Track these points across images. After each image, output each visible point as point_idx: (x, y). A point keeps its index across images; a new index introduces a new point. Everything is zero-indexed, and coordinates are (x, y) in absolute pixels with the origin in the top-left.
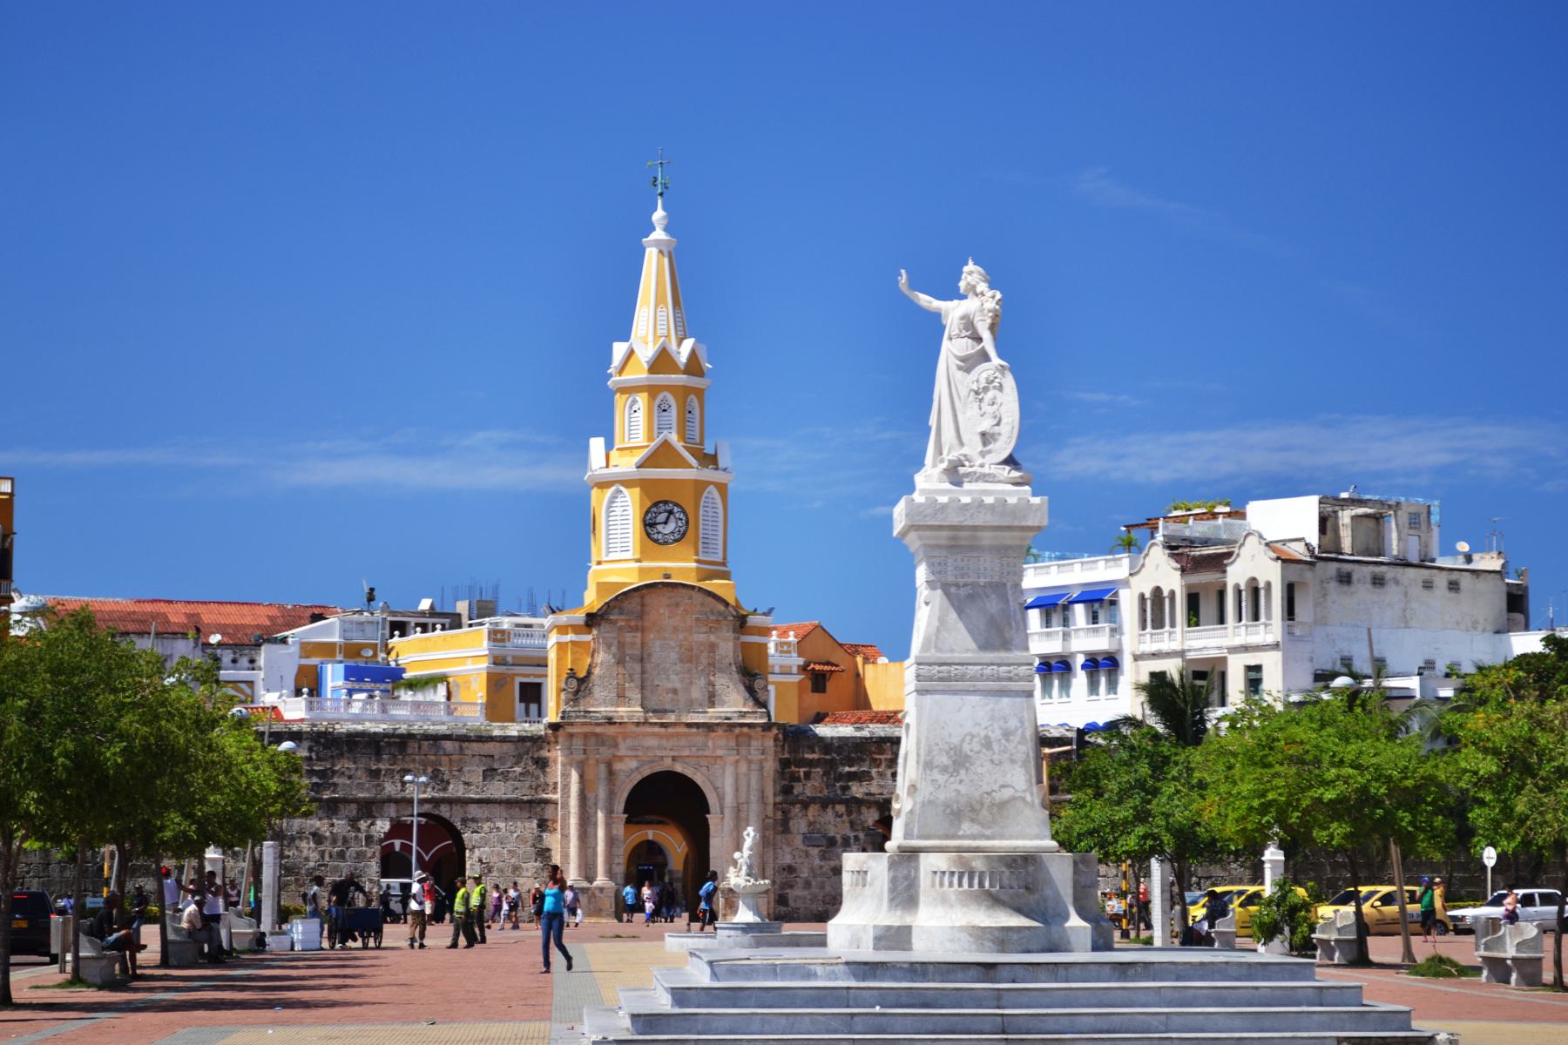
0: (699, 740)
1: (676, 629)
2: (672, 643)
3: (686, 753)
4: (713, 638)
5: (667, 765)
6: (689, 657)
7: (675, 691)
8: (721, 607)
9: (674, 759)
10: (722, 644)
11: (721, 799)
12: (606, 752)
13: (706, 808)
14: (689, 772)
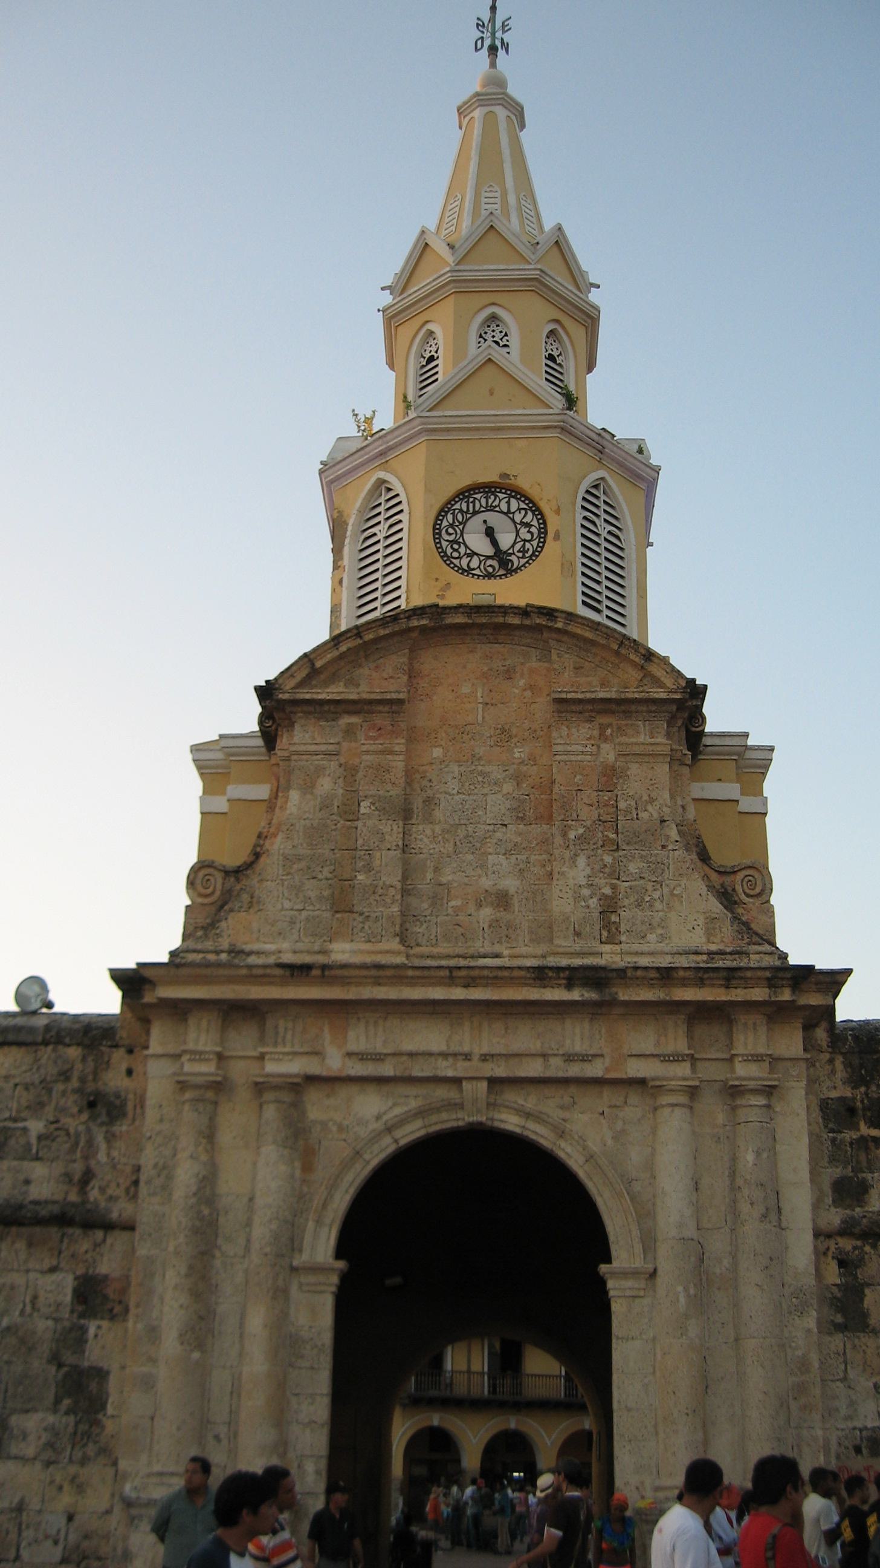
0: (576, 1036)
1: (504, 735)
2: (496, 773)
3: (533, 1069)
4: (609, 753)
5: (472, 1109)
6: (542, 807)
7: (502, 900)
8: (634, 675)
9: (494, 1082)
10: (634, 769)
11: (645, 1214)
12: (287, 1066)
13: (599, 1248)
14: (541, 1134)
